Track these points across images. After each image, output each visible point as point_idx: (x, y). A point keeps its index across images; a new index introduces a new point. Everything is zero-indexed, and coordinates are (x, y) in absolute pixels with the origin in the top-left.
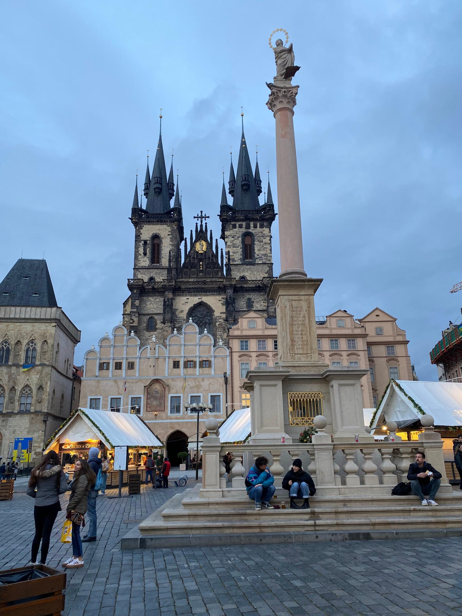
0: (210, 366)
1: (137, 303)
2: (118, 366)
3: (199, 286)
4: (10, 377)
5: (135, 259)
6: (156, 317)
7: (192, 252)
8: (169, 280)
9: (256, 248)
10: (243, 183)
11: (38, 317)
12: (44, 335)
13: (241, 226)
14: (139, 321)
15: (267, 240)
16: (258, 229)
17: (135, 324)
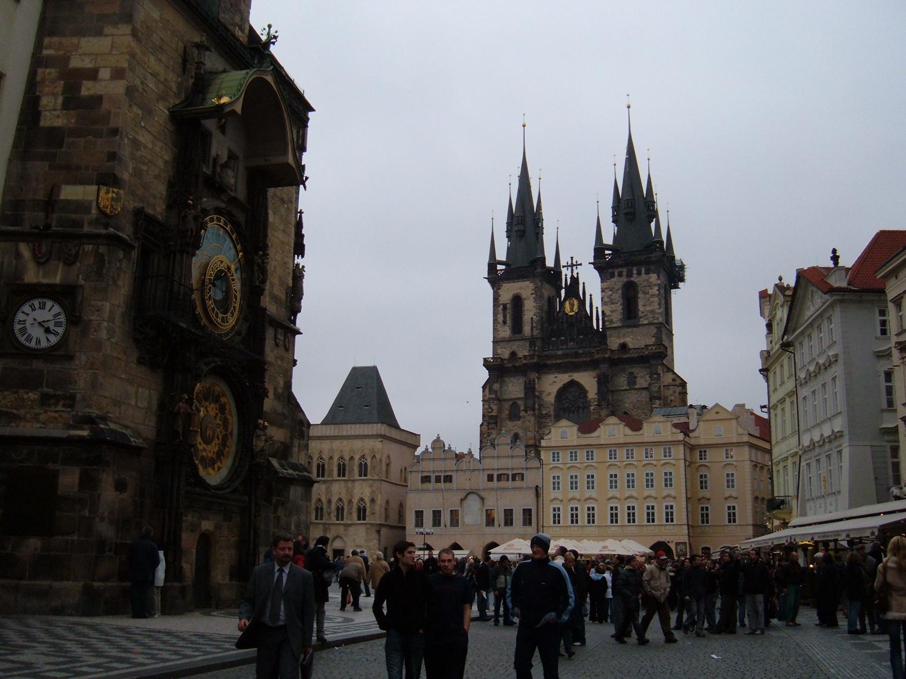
0: (523, 480)
1: (496, 386)
2: (438, 480)
3: (567, 360)
4: (347, 490)
5: (494, 329)
6: (519, 402)
7: (561, 314)
8: (532, 357)
9: (640, 303)
10: (626, 211)
11: (366, 433)
12: (372, 450)
13: (620, 275)
14: (500, 410)
15: (655, 291)
16: (643, 275)
17: (494, 414)
